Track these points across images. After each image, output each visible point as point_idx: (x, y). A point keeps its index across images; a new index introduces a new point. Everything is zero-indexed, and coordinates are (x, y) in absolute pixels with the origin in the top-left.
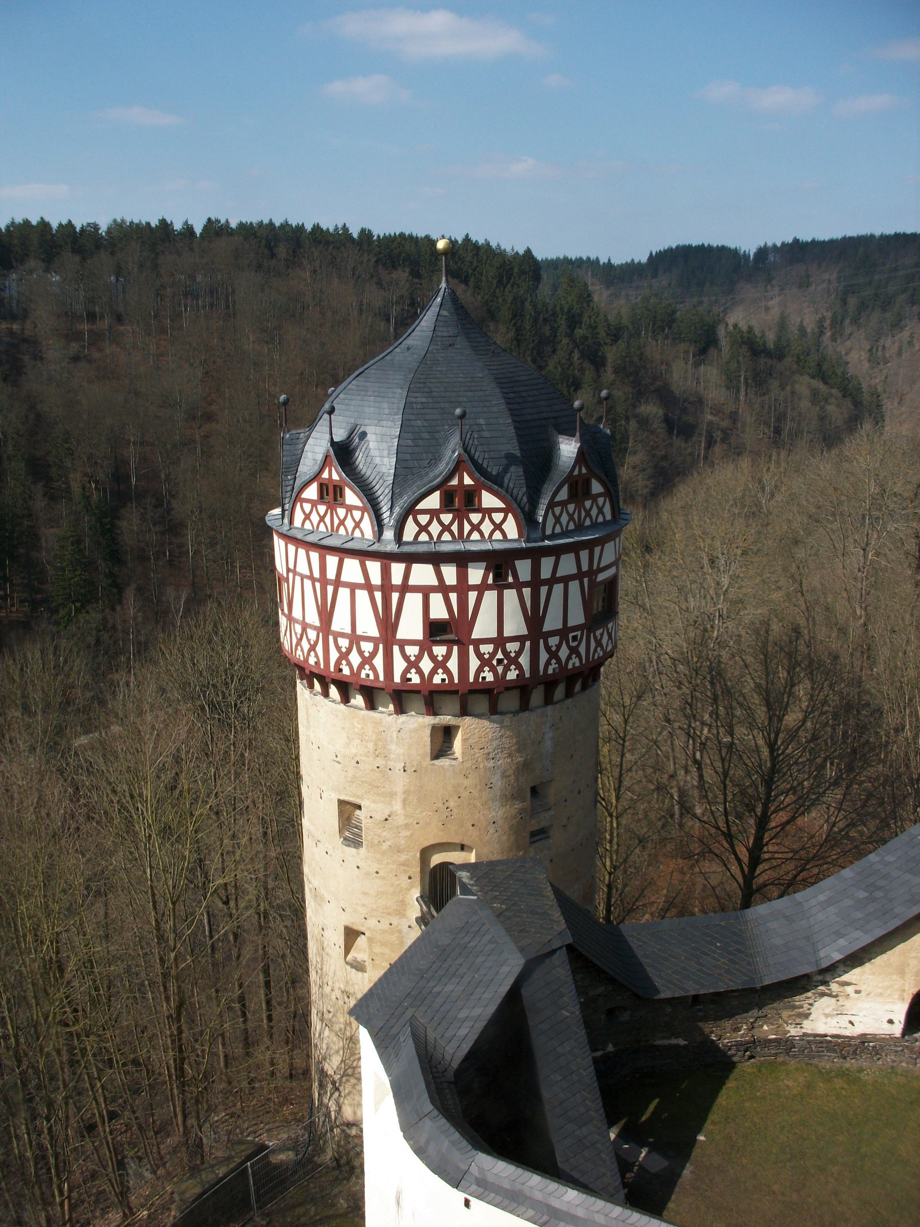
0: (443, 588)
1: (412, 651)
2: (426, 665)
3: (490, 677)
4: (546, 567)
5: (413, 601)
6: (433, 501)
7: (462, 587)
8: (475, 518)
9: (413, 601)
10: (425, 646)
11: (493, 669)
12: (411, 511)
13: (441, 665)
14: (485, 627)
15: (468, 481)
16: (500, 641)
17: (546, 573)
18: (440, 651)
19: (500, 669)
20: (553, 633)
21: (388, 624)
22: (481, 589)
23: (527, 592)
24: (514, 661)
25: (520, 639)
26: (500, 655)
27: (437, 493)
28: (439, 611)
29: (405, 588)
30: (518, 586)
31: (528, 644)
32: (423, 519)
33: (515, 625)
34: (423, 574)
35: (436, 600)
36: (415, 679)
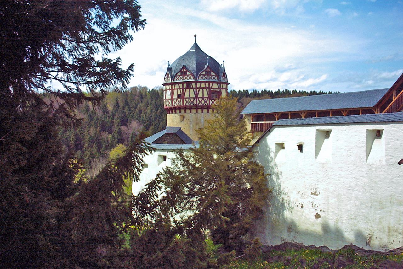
0: (180, 89)
1: (175, 100)
2: (177, 102)
3: (188, 105)
4: (198, 85)
5: (176, 91)
6: (179, 74)
7: (183, 88)
8: (186, 76)
9: (176, 91)
10: (177, 99)
11: (188, 103)
12: (176, 76)
13: (179, 102)
14: (187, 95)
15: (185, 70)
16: (190, 98)
17: (198, 86)
18: (179, 100)
19: (190, 103)
20: (200, 98)
21: (172, 96)
22: (186, 88)
23: (195, 90)
24: (193, 102)
25: (194, 98)
26: (190, 101)
27: (180, 73)
28: (179, 93)
29: (175, 89)
30: (193, 88)
31: (195, 99)
32: (177, 77)
33: (193, 95)
34: (177, 87)
35: (179, 90)
36: (176, 105)
